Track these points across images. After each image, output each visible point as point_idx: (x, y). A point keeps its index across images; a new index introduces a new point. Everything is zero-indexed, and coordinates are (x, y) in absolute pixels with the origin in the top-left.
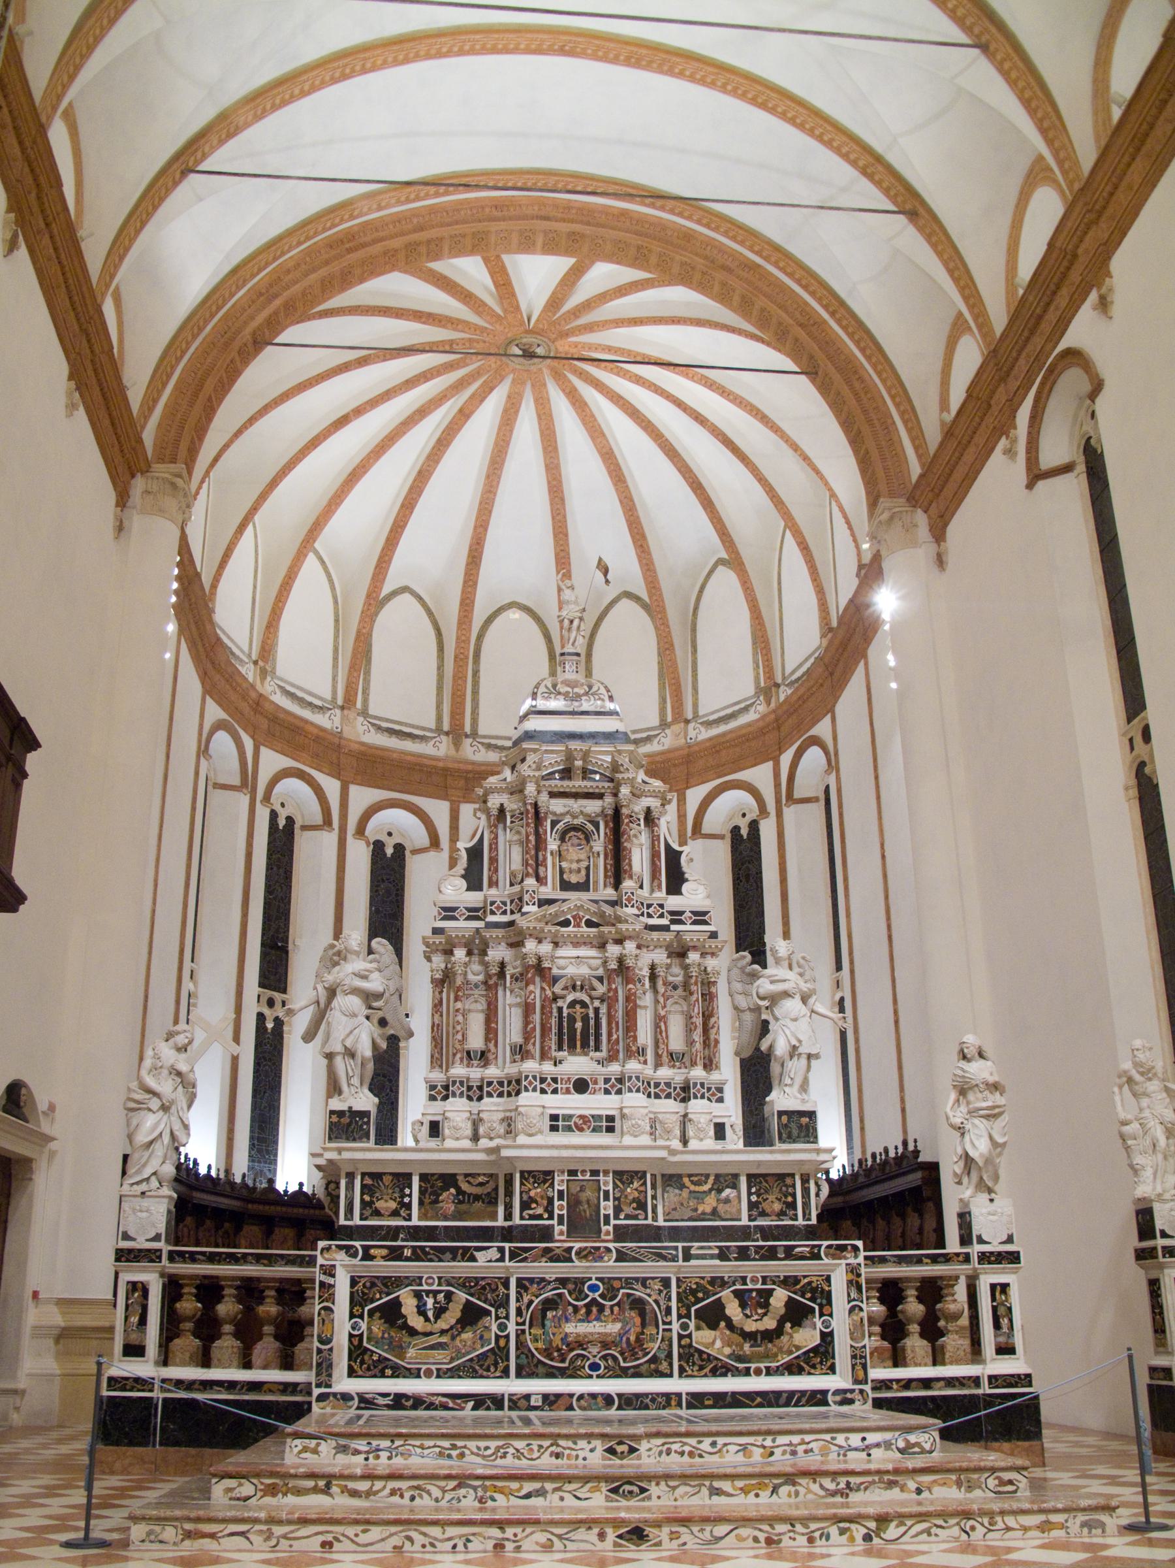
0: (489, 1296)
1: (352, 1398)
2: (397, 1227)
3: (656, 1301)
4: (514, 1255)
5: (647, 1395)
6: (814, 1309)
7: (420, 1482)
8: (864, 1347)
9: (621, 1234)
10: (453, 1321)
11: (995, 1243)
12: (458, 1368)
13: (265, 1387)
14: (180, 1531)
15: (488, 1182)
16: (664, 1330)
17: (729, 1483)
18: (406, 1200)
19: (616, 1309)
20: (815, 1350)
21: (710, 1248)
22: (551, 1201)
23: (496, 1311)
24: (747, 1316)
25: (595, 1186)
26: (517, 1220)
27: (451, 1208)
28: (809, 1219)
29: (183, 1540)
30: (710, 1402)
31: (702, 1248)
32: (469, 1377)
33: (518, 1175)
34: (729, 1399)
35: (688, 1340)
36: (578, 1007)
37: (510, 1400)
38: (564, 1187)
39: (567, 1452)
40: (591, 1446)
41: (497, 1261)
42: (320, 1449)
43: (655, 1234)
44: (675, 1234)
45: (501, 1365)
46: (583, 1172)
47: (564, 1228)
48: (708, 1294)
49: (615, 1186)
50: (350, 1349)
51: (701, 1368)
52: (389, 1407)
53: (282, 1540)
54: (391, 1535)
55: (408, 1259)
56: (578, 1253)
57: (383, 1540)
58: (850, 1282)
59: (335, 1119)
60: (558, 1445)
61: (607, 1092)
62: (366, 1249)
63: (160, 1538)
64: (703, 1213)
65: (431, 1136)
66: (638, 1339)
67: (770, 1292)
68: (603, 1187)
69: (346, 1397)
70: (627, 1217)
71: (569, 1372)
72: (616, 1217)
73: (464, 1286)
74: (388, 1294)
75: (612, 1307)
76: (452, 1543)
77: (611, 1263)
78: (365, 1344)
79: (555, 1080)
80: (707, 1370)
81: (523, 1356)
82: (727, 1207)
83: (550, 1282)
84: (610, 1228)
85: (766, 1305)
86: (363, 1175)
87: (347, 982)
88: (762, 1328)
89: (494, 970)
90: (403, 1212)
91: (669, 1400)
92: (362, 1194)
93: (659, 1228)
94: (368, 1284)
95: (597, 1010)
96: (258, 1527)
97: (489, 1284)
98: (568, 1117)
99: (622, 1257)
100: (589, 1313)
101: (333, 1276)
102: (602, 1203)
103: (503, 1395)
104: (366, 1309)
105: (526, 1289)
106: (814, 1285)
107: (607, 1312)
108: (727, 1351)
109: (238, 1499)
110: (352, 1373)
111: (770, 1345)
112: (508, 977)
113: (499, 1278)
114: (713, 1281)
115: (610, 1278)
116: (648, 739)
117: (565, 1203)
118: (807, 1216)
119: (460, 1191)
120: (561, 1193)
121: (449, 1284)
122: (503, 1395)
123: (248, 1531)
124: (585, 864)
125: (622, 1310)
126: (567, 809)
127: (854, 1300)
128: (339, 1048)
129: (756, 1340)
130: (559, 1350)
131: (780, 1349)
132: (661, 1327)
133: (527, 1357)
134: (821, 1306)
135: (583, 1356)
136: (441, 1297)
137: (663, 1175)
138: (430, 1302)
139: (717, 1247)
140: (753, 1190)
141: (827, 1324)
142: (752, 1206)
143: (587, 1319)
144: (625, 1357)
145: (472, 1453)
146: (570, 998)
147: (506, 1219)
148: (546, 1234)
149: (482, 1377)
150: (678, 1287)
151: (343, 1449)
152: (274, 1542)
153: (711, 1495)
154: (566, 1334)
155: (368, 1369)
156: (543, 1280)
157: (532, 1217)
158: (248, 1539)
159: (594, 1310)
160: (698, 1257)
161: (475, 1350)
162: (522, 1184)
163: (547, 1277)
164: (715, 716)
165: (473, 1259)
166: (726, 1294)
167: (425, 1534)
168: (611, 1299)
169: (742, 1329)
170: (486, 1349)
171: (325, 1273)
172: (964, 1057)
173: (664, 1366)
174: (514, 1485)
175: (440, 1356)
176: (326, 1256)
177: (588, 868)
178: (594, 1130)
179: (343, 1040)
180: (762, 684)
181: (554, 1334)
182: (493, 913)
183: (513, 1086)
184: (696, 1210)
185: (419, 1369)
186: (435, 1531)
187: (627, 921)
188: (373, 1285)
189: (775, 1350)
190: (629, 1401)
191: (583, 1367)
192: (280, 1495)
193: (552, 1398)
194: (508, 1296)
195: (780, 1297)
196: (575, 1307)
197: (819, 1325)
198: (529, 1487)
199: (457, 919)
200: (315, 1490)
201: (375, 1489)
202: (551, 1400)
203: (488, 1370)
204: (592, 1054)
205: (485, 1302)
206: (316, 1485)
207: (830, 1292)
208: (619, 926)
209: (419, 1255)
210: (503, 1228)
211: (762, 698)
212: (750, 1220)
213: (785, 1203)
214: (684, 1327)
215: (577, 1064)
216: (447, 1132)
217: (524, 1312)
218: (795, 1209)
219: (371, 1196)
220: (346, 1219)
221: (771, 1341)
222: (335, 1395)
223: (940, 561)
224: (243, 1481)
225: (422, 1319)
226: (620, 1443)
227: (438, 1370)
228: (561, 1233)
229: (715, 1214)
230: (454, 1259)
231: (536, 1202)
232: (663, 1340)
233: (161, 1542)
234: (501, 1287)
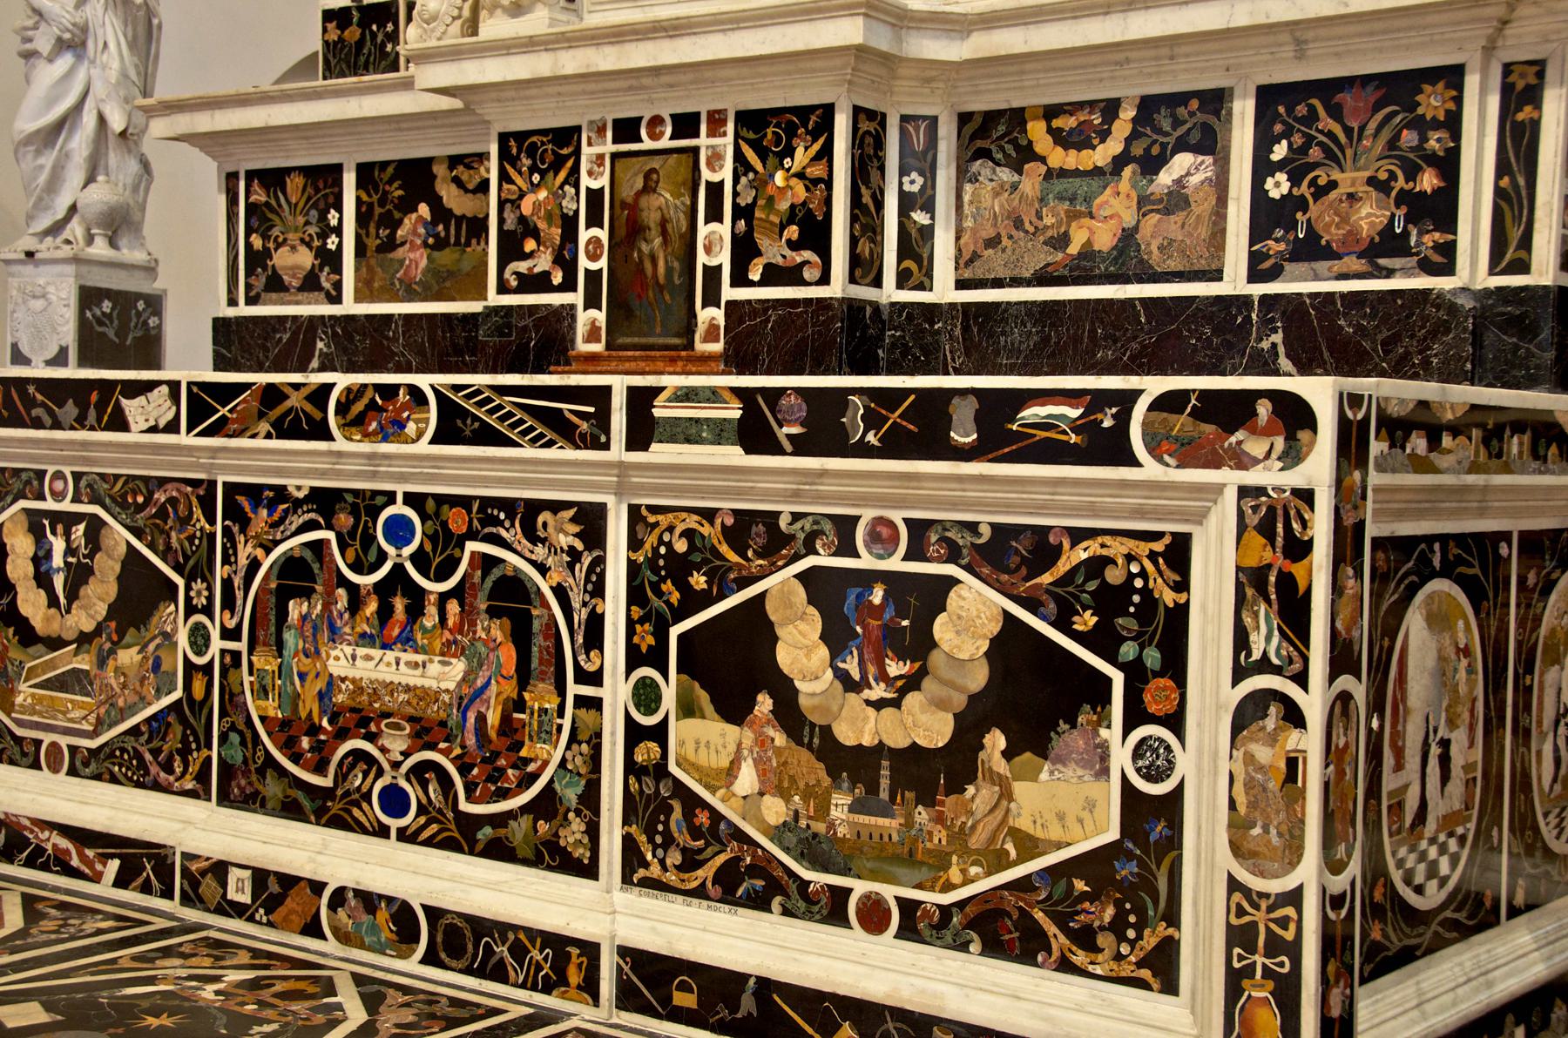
2: (311, 318)
3: (560, 592)
6: (1108, 681)
8: (1294, 897)
10: (101, 610)
16: (581, 701)
19: (453, 607)
20: (1095, 863)
23: (188, 588)
24: (849, 684)
25: (685, 173)
28: (1522, 267)
32: (130, 779)
33: (494, 149)
35: (654, 746)
37: (185, 872)
38: (603, 182)
43: (920, 336)
44: (980, 334)
46: (656, 121)
47: (600, 316)
51: (691, 862)
56: (342, 409)
58: (1251, 581)
64: (1087, 253)
67: (936, 593)
68: (707, 175)
70: (773, 276)
71: (335, 807)
72: (740, 279)
75: (444, 598)
77: (423, 447)
80: (706, 873)
81: (234, 738)
82: (1173, 226)
83: (297, 504)
84: (718, 314)
85: (920, 645)
88: (898, 741)
91: (561, 960)
93: (931, 311)
99: (455, 425)
100: (385, 613)
102: (703, 230)
105: (244, 523)
106: (1114, 576)
107: (430, 619)
108: (775, 810)
111: (922, 815)
114: (743, 527)
115: (441, 499)
117: (603, 234)
118: (1510, 247)
119: (441, 213)
120: (595, 196)
121: (95, 500)
125: (467, 613)
127: (1264, 666)
129: (873, 789)
130: (314, 730)
131: (960, 837)
132: (573, 689)
133: (243, 743)
134: (1136, 675)
137: (964, 118)
138: (58, 545)
139: (738, 392)
140: (1280, 152)
141: (1154, 761)
142: (1268, 216)
148: (544, 341)
149: (157, 786)
150: (634, 543)
154: (332, 682)
159: (395, 612)
160: (687, 432)
162: (504, 177)
163: (290, 483)
165: (119, 423)
166: (780, 585)
168: (441, 577)
169: (827, 731)
170: (166, 701)
175: (77, 708)
181: (302, 676)
184: (1062, 241)
189: (940, 835)
190: (461, 938)
191: (367, 797)
195: (974, 612)
196: (353, 589)
197: (1121, 758)
202: (276, 891)
203: (168, 768)
205: (165, 560)
207: (1182, 611)
212: (1254, 276)
213: (1404, 198)
214: (646, 696)
217: (239, 594)
219: (265, 237)
221: (927, 798)
228: (593, 336)
229: (1126, 261)
230: (80, 423)
232: (573, 739)
234: (198, 512)
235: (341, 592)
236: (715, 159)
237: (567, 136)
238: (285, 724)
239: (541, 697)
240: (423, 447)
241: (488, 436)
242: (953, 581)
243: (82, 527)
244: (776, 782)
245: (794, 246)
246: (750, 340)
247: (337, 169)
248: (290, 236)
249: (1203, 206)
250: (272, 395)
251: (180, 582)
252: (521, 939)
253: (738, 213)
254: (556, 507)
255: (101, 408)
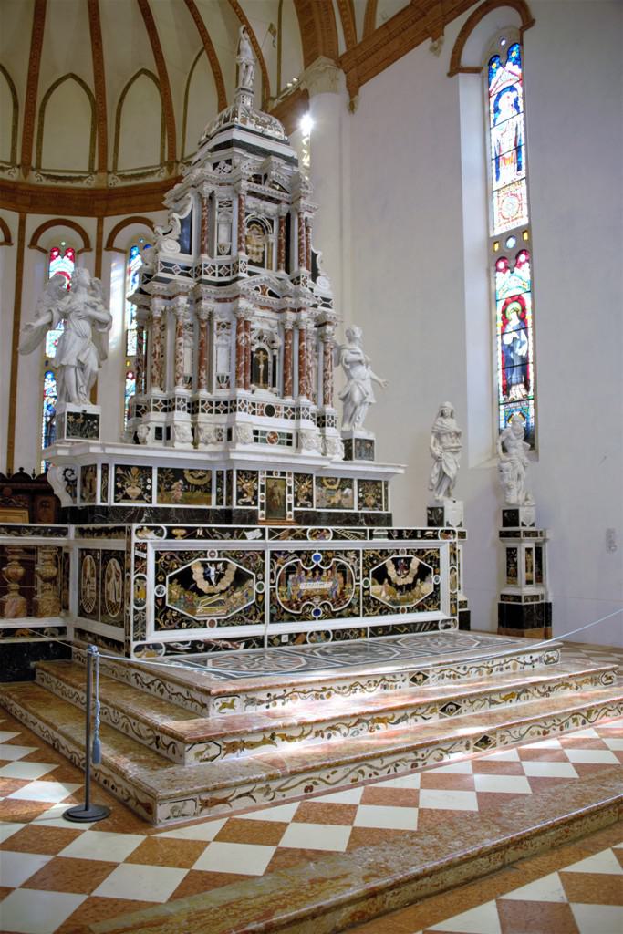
0: (252, 564)
1: (162, 648)
3: (352, 566)
4: (272, 534)
5: (348, 630)
7: (334, 723)
9: (302, 518)
10: (229, 584)
11: (455, 526)
12: (231, 618)
13: (18, 633)
14: (199, 803)
15: (205, 476)
16: (357, 586)
17: (498, 696)
18: (148, 487)
19: (330, 572)
20: (431, 596)
21: (383, 530)
22: (256, 492)
24: (399, 575)
26: (235, 507)
27: (180, 494)
29: (201, 810)
30: (380, 632)
31: (379, 530)
32: (239, 624)
33: (235, 473)
34: (391, 630)
36: (261, 353)
37: (269, 640)
38: (264, 483)
39: (390, 684)
40: (403, 678)
41: (260, 538)
42: (234, 704)
45: (260, 615)
46: (276, 472)
47: (264, 512)
48: (379, 561)
49: (295, 483)
50: (156, 608)
51: (375, 610)
52: (188, 651)
53: (277, 793)
54: (351, 772)
55: (200, 538)
56: (311, 534)
57: (345, 777)
58: (451, 553)
59: (72, 419)
60: (385, 680)
61: (286, 417)
62: (170, 529)
63: (182, 812)
64: (334, 504)
65: (156, 438)
66: (342, 593)
68: (288, 485)
69: (156, 647)
70: (302, 506)
72: (295, 506)
73: (235, 557)
74: (183, 565)
75: (327, 570)
76: (387, 770)
77: (330, 541)
78: (167, 604)
79: (254, 405)
83: (291, 554)
84: (292, 513)
85: (408, 568)
86: (116, 466)
87: (81, 308)
89: (204, 317)
90: (146, 497)
91: (360, 632)
92: (116, 481)
94: (168, 557)
95: (274, 357)
96: (260, 786)
97: (252, 556)
98: (264, 433)
99: (336, 536)
100: (314, 575)
101: (145, 551)
102: (288, 496)
103: (263, 637)
104: (168, 577)
105: (276, 559)
107: (325, 574)
108: (388, 598)
109: (207, 760)
110: (158, 627)
112: (215, 324)
113: (259, 551)
115: (326, 551)
116: (80, 179)
117: (264, 494)
119: (185, 480)
120: (262, 486)
121: (226, 556)
122: (263, 637)
123: (252, 791)
124: (261, 250)
125: (333, 572)
126: (256, 206)
128: (74, 362)
130: (296, 602)
131: (414, 595)
132: (355, 583)
134: (435, 568)
135: (311, 605)
136: (220, 565)
138: (213, 570)
139: (388, 530)
141: (437, 580)
142: (360, 500)
143: (314, 578)
144: (335, 606)
145: (336, 692)
146: (257, 346)
147: (217, 504)
149: (247, 624)
150: (364, 556)
151: (251, 701)
152: (271, 796)
153: (490, 704)
154: (301, 591)
155: (170, 623)
156: (286, 552)
157: (245, 504)
158: (252, 797)
160: (378, 537)
161: (243, 604)
162: (238, 479)
163: (289, 550)
164: (130, 173)
165: (244, 537)
166: (388, 561)
167: (371, 767)
169: (396, 584)
170: (250, 603)
171: (139, 550)
172: (442, 415)
173: (355, 610)
174: (390, 716)
175: (220, 610)
176: (140, 535)
177: (263, 253)
178: (280, 443)
179: (78, 355)
180: (166, 159)
182: (206, 273)
183: (230, 407)
184: (330, 501)
185: (205, 621)
186: (377, 763)
187: (304, 297)
188: (172, 557)
190: (339, 634)
192: (239, 751)
193: (295, 636)
194: (264, 564)
195: (416, 562)
196: (306, 571)
198: (399, 715)
199: (173, 273)
200: (264, 742)
201: (305, 733)
202: (294, 637)
203: (251, 619)
204: (270, 388)
206: (264, 738)
208: (302, 299)
209: (208, 535)
210: (216, 510)
211: (165, 168)
213: (377, 499)
214: (366, 583)
215: (264, 395)
216: (177, 437)
218: (381, 503)
219: (123, 483)
220: (102, 501)
221: (410, 591)
222: (148, 646)
223: (352, 107)
224: (210, 744)
225: (207, 582)
226: (419, 674)
227: (218, 620)
228: (262, 516)
229: (339, 506)
230: (231, 538)
231: (247, 493)
232: (355, 592)
233: (184, 815)
234: (259, 558)
235: (303, 572)
236: (290, 481)
237: (255, 472)
238: (289, 602)
239: (348, 586)
240: (330, 541)
241: (343, 538)
242: (412, 558)
243: (221, 564)
244: (388, 594)
245: (306, 500)
246: (302, 518)
247: (150, 469)
248: (133, 485)
249: (351, 497)
250: (292, 531)
251: (254, 574)
252: (352, 631)
253: (295, 493)
254: (351, 551)
255: (238, 534)
